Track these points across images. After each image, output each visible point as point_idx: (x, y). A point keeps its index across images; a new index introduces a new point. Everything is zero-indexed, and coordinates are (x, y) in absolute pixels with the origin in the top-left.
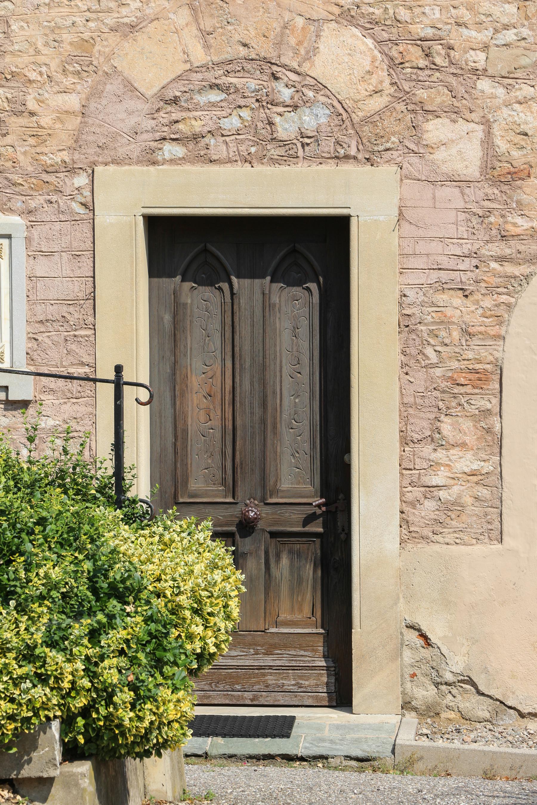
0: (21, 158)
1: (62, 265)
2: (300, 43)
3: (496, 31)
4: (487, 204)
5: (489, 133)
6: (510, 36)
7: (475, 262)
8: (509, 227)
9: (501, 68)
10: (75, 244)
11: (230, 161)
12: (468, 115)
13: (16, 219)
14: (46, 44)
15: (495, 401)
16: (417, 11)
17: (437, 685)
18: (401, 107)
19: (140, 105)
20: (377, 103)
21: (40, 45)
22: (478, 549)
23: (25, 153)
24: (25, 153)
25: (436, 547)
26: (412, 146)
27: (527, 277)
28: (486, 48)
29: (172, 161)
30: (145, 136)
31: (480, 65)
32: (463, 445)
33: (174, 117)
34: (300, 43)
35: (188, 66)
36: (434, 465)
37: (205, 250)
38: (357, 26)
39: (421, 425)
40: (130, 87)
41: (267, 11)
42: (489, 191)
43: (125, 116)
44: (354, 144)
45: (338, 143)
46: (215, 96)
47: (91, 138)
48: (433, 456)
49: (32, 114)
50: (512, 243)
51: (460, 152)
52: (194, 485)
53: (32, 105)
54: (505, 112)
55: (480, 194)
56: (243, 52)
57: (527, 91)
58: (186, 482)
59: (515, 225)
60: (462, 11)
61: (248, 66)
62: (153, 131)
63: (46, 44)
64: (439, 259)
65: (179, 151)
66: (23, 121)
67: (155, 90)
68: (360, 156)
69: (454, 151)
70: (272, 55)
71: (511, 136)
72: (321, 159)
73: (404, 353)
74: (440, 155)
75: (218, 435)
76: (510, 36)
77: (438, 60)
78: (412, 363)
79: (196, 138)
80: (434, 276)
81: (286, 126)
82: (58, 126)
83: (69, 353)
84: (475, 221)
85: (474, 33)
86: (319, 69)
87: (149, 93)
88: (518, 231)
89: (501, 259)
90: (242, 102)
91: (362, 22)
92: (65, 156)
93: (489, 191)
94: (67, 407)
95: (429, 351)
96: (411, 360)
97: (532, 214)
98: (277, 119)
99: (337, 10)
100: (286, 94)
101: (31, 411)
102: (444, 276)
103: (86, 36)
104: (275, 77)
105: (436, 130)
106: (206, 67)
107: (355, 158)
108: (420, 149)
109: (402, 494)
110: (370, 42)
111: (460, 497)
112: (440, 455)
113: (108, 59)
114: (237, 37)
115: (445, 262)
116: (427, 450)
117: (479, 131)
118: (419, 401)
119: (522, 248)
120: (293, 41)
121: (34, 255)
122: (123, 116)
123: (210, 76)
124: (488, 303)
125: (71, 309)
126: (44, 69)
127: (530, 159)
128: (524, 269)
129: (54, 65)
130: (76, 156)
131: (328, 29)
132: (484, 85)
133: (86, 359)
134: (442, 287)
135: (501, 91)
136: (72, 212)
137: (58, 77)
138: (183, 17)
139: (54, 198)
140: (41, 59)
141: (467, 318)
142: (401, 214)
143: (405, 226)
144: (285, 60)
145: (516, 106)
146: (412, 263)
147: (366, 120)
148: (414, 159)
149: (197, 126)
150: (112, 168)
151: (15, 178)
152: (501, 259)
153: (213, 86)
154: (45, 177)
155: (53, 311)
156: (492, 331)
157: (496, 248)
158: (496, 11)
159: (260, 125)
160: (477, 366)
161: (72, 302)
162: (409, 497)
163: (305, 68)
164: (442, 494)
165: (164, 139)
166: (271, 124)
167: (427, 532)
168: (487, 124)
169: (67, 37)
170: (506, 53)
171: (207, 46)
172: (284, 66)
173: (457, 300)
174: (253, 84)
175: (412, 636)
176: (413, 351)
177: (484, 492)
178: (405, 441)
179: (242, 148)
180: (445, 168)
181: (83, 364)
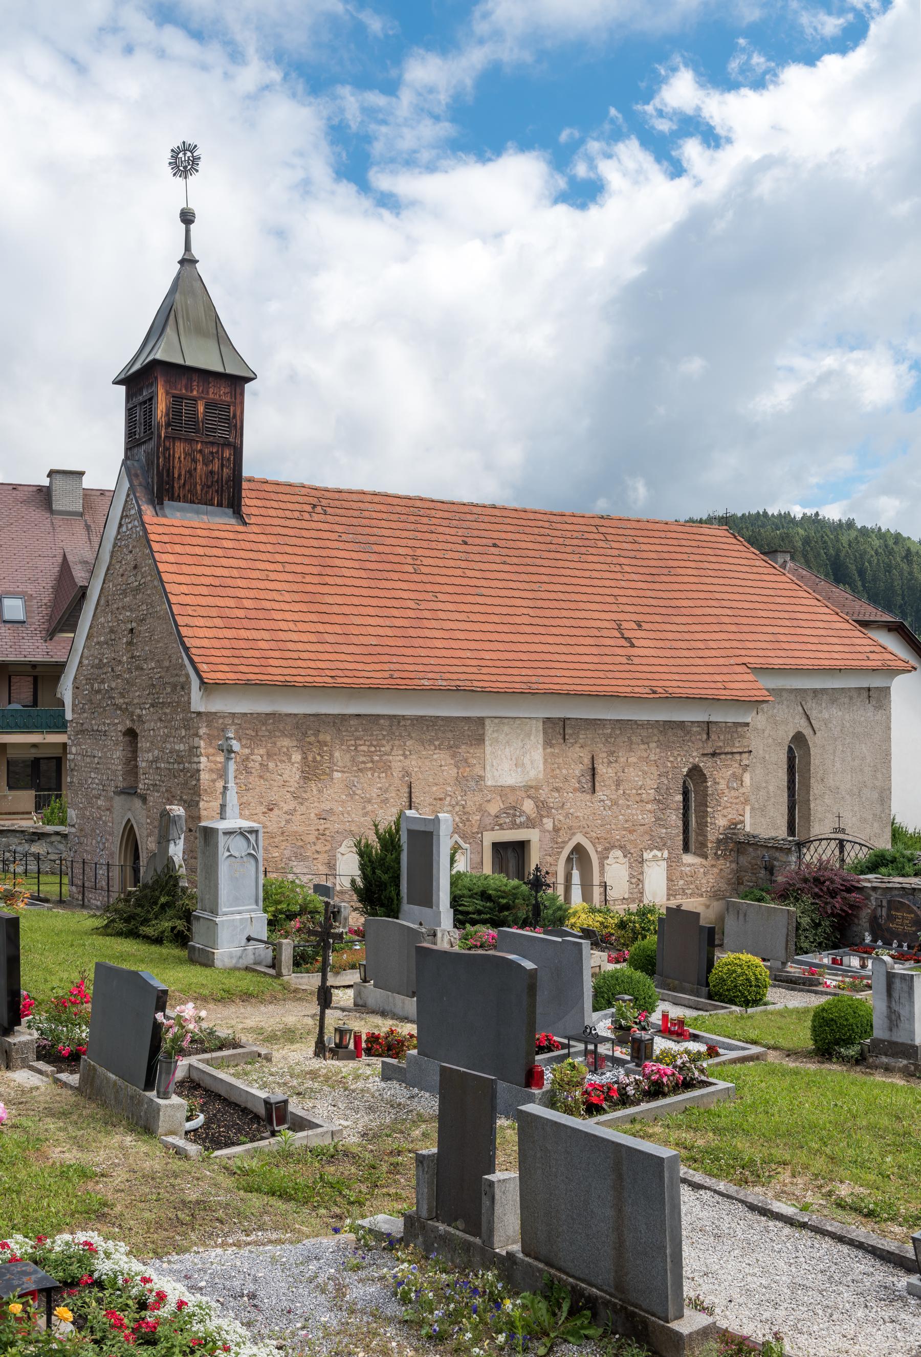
20: (534, 815)
43: (488, 821)
86: (524, 808)
105: (545, 820)
108: (542, 824)
138: (499, 798)
157: (556, 846)
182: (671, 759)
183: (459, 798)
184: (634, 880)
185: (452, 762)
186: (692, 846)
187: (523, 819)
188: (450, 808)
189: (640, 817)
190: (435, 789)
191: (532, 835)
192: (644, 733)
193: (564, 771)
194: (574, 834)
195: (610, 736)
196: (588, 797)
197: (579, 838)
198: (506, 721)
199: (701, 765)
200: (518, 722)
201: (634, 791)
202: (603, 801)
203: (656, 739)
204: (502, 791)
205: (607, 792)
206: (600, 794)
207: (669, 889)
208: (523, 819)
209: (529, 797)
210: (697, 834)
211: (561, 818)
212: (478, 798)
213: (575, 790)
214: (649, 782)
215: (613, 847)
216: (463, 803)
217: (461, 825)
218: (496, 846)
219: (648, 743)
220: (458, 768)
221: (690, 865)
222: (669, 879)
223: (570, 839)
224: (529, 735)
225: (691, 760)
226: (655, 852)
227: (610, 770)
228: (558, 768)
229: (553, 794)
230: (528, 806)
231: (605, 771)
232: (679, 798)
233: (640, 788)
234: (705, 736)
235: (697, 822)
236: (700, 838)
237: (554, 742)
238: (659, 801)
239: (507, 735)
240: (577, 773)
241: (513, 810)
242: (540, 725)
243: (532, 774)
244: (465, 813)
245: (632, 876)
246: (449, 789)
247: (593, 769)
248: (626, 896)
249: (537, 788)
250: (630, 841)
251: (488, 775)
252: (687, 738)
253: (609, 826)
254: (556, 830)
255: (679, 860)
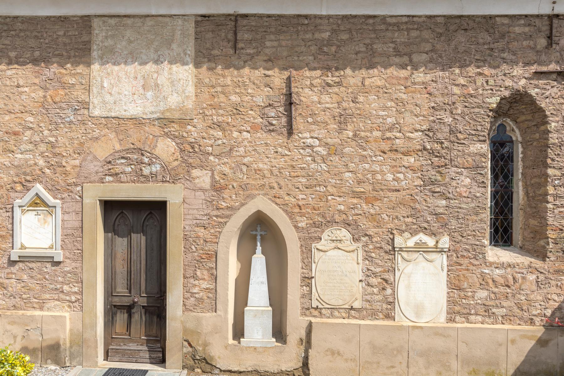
0: (60, 181)
1: (73, 216)
2: (151, 143)
3: (215, 140)
4: (212, 197)
5: (213, 174)
6: (220, 142)
7: (208, 217)
8: (220, 206)
9: (217, 152)
10: (77, 209)
11: (128, 182)
12: (206, 168)
13: (58, 201)
14: (69, 144)
15: (214, 264)
16: (189, 133)
17: (194, 360)
18: (184, 165)
19: (99, 163)
20: (176, 163)
21: (67, 144)
22: (208, 315)
23: (61, 179)
24: (61, 179)
25: (195, 314)
26: (188, 178)
27: (226, 223)
28: (212, 146)
29: (109, 182)
30: (100, 174)
31: (210, 152)
32: (204, 279)
33: (110, 167)
34: (151, 143)
35: (114, 151)
36: (195, 286)
37: (122, 212)
38: (170, 138)
39: (190, 272)
40: (95, 158)
41: (140, 133)
42: (213, 193)
44: (168, 177)
45: (163, 176)
46: (123, 161)
47: (83, 174)
48: (194, 283)
49: (64, 167)
50: (221, 211)
51: (204, 180)
52: (119, 289)
53: (64, 164)
54: (218, 167)
55: (210, 194)
56: (132, 146)
57: (226, 160)
58: (115, 289)
59: (222, 205)
60: (204, 134)
61: (134, 151)
62: (103, 172)
63: (69, 144)
64: (196, 216)
65: (111, 179)
66: (61, 169)
67: (103, 158)
68: (170, 181)
69: (201, 180)
70: (142, 147)
71: (220, 175)
72: (157, 182)
73: (184, 248)
74: (197, 181)
75: (126, 273)
76: (220, 142)
77: (196, 150)
78: (187, 251)
79: (117, 174)
80: (195, 221)
81: (146, 171)
82: (72, 170)
83: (74, 246)
84: (208, 203)
85: (208, 141)
86: (157, 152)
87: (101, 160)
88: (223, 207)
89: (217, 216)
90: (132, 163)
91: (171, 137)
92: (74, 180)
93: (213, 193)
94: (73, 264)
95: (193, 247)
96: (187, 250)
97: (227, 201)
98: (143, 168)
99: (163, 133)
100: (146, 160)
101: (62, 265)
102: (198, 221)
103: (82, 141)
104: (142, 155)
105: (196, 173)
106: (120, 151)
107: (169, 182)
108: (191, 179)
109: (184, 295)
110: (174, 143)
111: (203, 296)
112: (196, 282)
113: (89, 148)
114: (130, 141)
115: (198, 217)
116: (192, 280)
117: (210, 173)
118: (189, 264)
119: (224, 213)
120: (149, 143)
121: (64, 213)
122: (93, 167)
123: (122, 154)
124: (212, 231)
125: (75, 231)
126: (68, 152)
127: (227, 183)
128: (225, 220)
129: (71, 151)
130: (78, 180)
131: (160, 139)
132: (211, 158)
133: (80, 248)
134: (197, 225)
135: (217, 160)
136: (76, 199)
137: (73, 155)
138: (112, 136)
139: (70, 194)
140: (67, 149)
141: (205, 236)
142: (184, 200)
143: (186, 205)
144: (146, 149)
145: (222, 165)
146: (188, 217)
147: (172, 169)
148: (188, 182)
149: (117, 171)
150: (89, 184)
151: (58, 187)
152: (217, 216)
153: (123, 158)
154: (68, 187)
155: (70, 232)
156: (215, 240)
157: (215, 213)
158: (215, 134)
159: (138, 170)
160: (209, 252)
161: (76, 229)
162: (186, 296)
163: (153, 151)
164: (197, 296)
165: (106, 175)
166: (141, 170)
167: (191, 308)
168: (213, 171)
169: (76, 142)
170: (218, 147)
171: (121, 144)
172: (146, 151)
173: (203, 230)
174: (135, 157)
175: (186, 344)
176: (187, 247)
177: (211, 295)
178: (185, 277)
179: (132, 178)
180: (198, 186)
181: (78, 250)
182: (462, 81)
183: (46, 133)
184: (374, 281)
185: (37, 81)
186: (518, 234)
187: (156, 168)
188: (31, 147)
189: (390, 177)
190: (7, 118)
191: (172, 195)
192: (401, 38)
193: (234, 98)
194: (251, 197)
195: (329, 43)
196: (281, 140)
197: (261, 204)
198: (129, 21)
199: (533, 92)
200: (150, 22)
201: (377, 134)
202: (311, 147)
203: (428, 47)
204: (118, 124)
205: (322, 133)
206: (305, 134)
207: (451, 302)
208: (156, 168)
209: (167, 135)
210: (527, 216)
211: (226, 170)
212: (78, 134)
213: (255, 128)
214: (409, 119)
215: (332, 222)
216: (52, 139)
217: (48, 171)
218: (109, 206)
219: (409, 55)
220: (45, 89)
221: (501, 266)
222: (454, 285)
223: (242, 205)
224: (169, 43)
225: (509, 83)
226: (422, 237)
227: (326, 98)
228: (223, 93)
229: (212, 132)
230: (166, 148)
231: (316, 99)
232: (485, 148)
233: (390, 129)
234: (543, 42)
235: (527, 194)
236: (533, 222)
237: (216, 52)
238: (431, 152)
239: (130, 42)
240: (260, 100)
241: (137, 155)
242: (191, 27)
243: (174, 100)
244: (55, 155)
245: (369, 273)
246: (31, 119)
247: (289, 95)
248: (356, 305)
249: (183, 122)
250: (372, 217)
251: (95, 100)
252: (500, 45)
253: (322, 189)
254: (217, 188)
255: (478, 253)
